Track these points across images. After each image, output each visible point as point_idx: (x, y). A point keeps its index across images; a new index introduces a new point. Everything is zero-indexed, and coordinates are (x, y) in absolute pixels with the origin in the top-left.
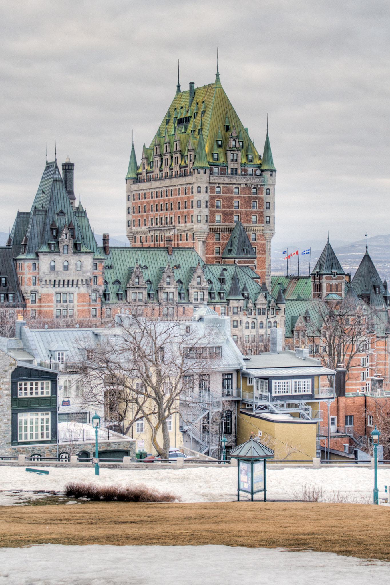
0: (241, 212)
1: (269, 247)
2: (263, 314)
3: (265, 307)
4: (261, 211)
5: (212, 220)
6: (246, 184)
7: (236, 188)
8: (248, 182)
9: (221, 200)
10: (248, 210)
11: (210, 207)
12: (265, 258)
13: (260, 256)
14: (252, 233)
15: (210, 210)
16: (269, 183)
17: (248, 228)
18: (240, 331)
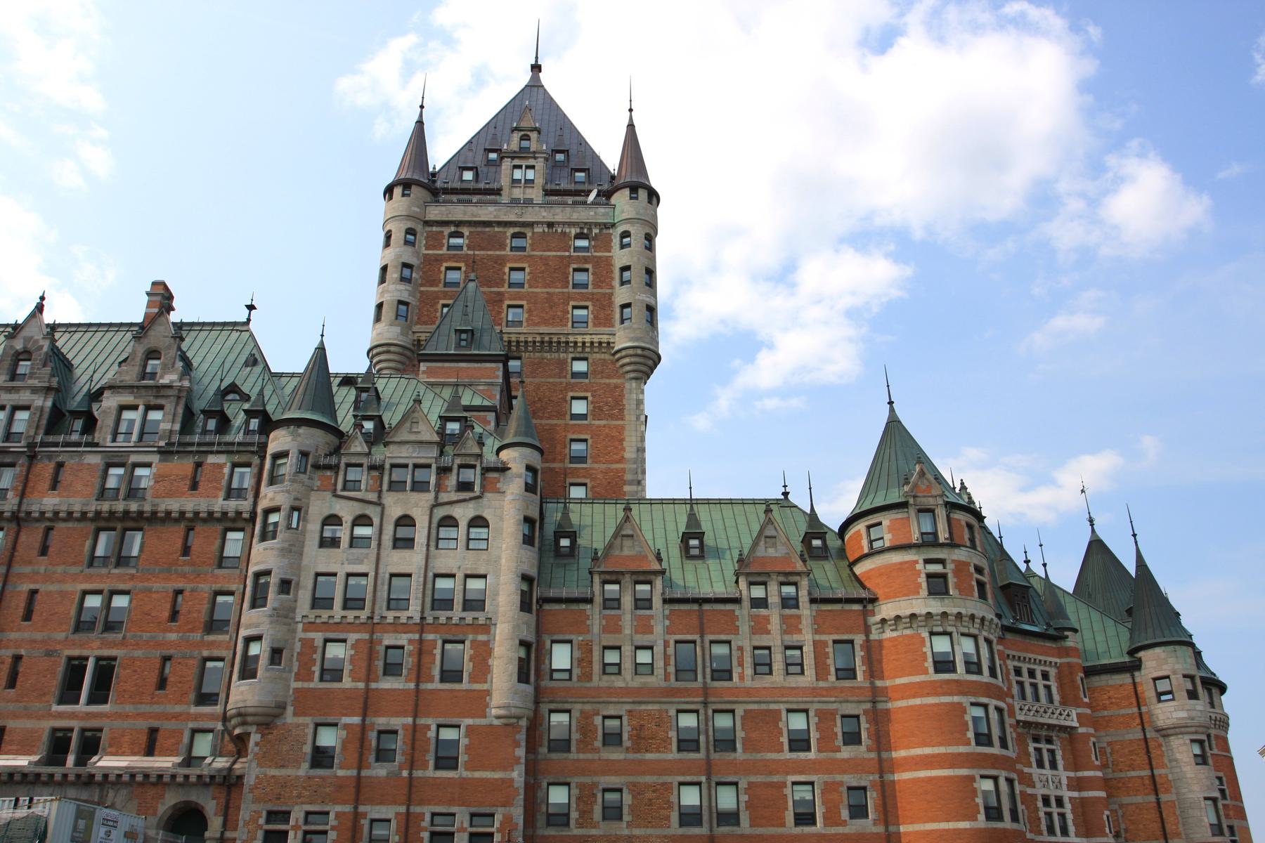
0: (530, 297)
1: (634, 396)
2: (413, 490)
3: (429, 456)
4: (604, 294)
5: (425, 319)
6: (550, 225)
7: (514, 236)
8: (559, 218)
9: (462, 265)
10: (557, 290)
11: (422, 285)
12: (621, 429)
13: (603, 423)
14: (571, 355)
15: (421, 292)
16: (625, 216)
17: (555, 339)
18: (294, 551)
